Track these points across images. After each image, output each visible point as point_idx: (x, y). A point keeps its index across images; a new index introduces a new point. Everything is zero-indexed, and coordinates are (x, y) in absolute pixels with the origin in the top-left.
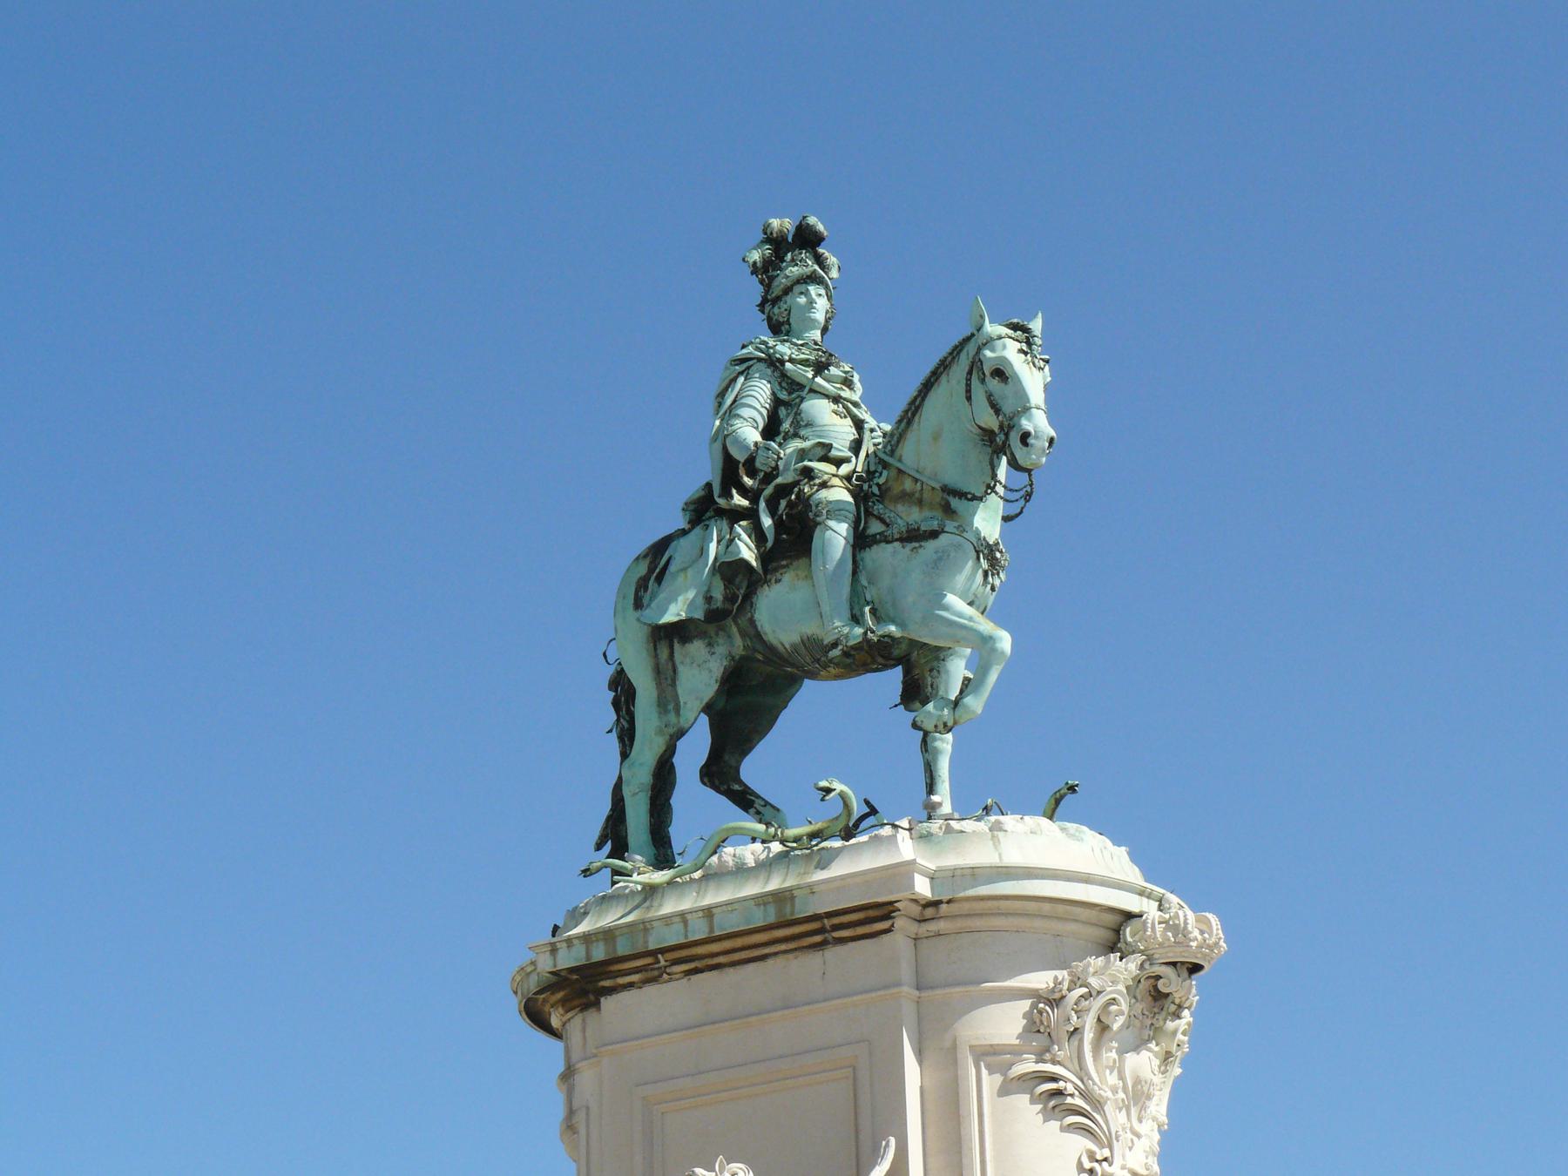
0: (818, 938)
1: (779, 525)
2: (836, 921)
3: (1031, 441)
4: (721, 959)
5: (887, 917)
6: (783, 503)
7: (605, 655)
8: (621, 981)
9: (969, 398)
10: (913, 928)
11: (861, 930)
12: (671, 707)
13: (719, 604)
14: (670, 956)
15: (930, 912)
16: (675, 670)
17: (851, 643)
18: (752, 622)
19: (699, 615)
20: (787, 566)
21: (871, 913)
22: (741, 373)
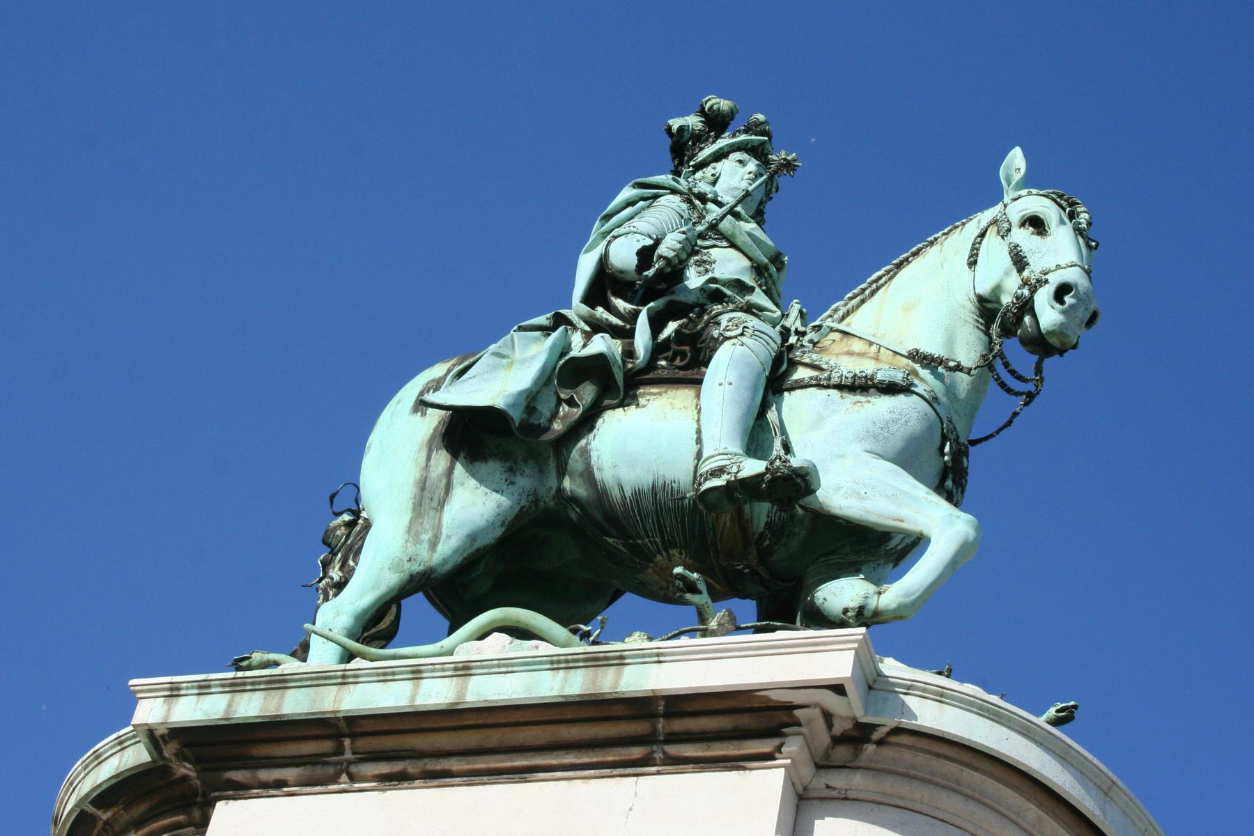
0: (636, 752)
1: (658, 349)
2: (678, 725)
3: (1068, 299)
4: (455, 764)
5: (774, 732)
6: (672, 327)
7: (332, 498)
8: (265, 775)
9: (972, 263)
10: (807, 771)
11: (718, 750)
12: (426, 537)
13: (542, 421)
14: (363, 743)
15: (842, 752)
16: (448, 488)
17: (742, 475)
18: (585, 452)
19: (517, 415)
20: (660, 394)
21: (745, 721)
22: (644, 199)
